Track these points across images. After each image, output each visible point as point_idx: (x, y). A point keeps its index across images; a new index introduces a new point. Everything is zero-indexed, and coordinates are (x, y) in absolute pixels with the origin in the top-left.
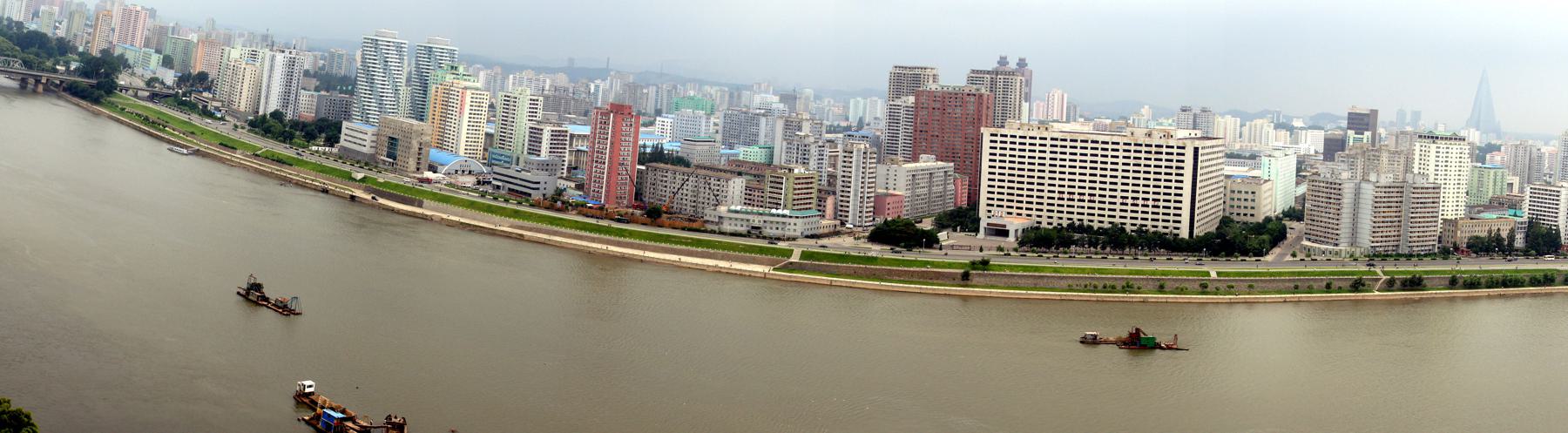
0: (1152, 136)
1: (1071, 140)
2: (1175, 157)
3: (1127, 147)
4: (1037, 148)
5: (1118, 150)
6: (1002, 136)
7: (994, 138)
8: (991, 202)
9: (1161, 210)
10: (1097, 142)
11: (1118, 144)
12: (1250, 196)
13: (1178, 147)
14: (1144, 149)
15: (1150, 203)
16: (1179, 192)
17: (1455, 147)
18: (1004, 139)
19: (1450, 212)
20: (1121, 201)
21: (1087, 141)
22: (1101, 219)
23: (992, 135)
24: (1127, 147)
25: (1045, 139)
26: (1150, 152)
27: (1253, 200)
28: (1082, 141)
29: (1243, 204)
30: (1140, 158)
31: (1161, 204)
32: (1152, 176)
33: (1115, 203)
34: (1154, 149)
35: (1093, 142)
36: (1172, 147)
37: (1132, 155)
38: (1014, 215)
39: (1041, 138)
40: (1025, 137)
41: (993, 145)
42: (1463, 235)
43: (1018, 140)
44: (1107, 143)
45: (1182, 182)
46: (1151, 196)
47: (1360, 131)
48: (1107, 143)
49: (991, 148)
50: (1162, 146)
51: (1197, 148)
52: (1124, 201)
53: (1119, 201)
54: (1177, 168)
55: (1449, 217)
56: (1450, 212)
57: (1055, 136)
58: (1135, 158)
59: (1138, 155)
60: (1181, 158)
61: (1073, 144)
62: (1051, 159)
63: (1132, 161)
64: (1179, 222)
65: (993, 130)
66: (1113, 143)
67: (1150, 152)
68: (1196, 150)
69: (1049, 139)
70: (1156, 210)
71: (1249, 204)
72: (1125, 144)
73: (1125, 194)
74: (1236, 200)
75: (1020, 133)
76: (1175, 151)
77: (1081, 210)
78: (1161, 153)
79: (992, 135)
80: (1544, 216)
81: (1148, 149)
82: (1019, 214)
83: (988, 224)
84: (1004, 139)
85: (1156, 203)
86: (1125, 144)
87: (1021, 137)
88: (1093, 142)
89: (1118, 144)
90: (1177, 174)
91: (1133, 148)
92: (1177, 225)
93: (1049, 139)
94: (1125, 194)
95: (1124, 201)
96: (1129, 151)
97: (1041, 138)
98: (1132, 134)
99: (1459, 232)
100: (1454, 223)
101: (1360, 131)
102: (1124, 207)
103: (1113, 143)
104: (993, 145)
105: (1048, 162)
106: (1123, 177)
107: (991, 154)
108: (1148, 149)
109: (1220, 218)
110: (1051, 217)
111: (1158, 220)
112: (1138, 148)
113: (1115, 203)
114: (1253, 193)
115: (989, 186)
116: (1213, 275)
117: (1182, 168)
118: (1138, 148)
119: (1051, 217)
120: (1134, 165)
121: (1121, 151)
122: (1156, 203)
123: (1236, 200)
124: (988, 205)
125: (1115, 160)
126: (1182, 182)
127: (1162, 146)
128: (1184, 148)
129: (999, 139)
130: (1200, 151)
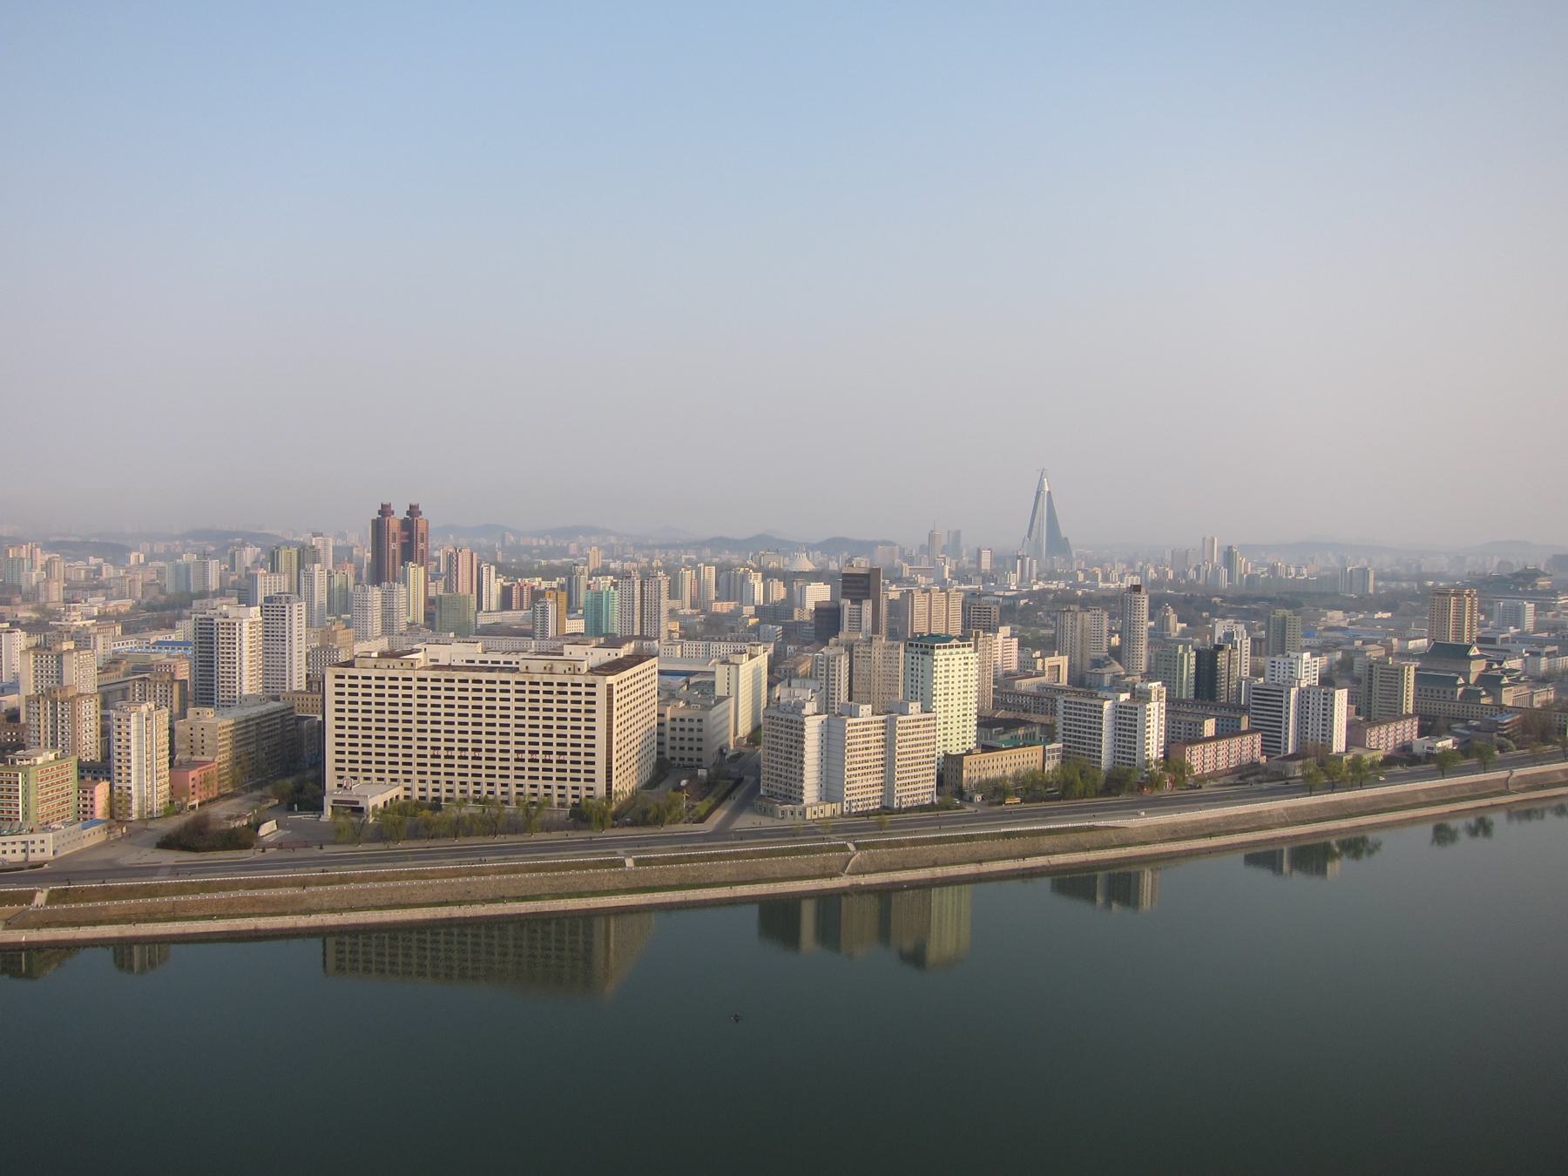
0: (554, 671)
1: (447, 681)
2: (583, 698)
3: (520, 687)
4: (400, 692)
5: (508, 691)
6: (350, 677)
7: (340, 681)
8: (340, 765)
9: (569, 766)
10: (480, 682)
11: (508, 683)
12: (695, 725)
13: (587, 685)
14: (542, 688)
15: (554, 757)
16: (590, 742)
17: (957, 657)
18: (353, 682)
19: (954, 742)
20: (515, 756)
21: (466, 681)
22: (491, 780)
23: (337, 677)
24: (520, 687)
25: (410, 679)
26: (551, 693)
27: (700, 730)
28: (460, 681)
29: (686, 735)
30: (538, 701)
31: (569, 758)
32: (555, 723)
33: (508, 760)
34: (555, 688)
35: (475, 681)
36: (580, 685)
37: (527, 696)
38: (375, 780)
39: (404, 679)
40: (383, 679)
41: (340, 690)
42: (972, 775)
43: (373, 682)
44: (494, 682)
45: (593, 729)
46: (555, 749)
47: (857, 601)
48: (494, 682)
49: (337, 694)
50: (566, 685)
51: (612, 685)
52: (520, 756)
53: (512, 755)
54: (587, 711)
55: (954, 753)
56: (954, 742)
57: (423, 674)
58: (531, 700)
59: (534, 696)
60: (591, 698)
61: (449, 685)
62: (419, 705)
63: (527, 705)
64: (593, 780)
65: (340, 671)
66: (502, 682)
67: (551, 693)
68: (610, 687)
69: (415, 679)
70: (562, 766)
71: (695, 735)
72: (517, 683)
73: (520, 747)
74: (678, 730)
75: (374, 673)
76: (583, 689)
77: (463, 771)
78: (566, 693)
79: (337, 677)
80: (1085, 744)
81: (547, 688)
82: (379, 779)
83: (335, 801)
84: (353, 682)
85: (562, 758)
86: (517, 683)
87: (377, 678)
88: (475, 681)
89: (508, 683)
90: (587, 720)
91: (527, 687)
92: (591, 784)
93: (415, 679)
94: (520, 747)
95: (520, 756)
96: (523, 692)
97: (404, 679)
98: (527, 668)
99: (965, 772)
100: (958, 759)
101: (857, 601)
102: (520, 764)
103: (502, 682)
104: (340, 690)
105: (415, 709)
106: (517, 726)
107: (337, 702)
108: (547, 688)
109: (655, 759)
110: (424, 781)
111: (565, 779)
112: (535, 688)
113: (508, 760)
114: (699, 721)
115: (337, 744)
116: (629, 862)
117: (594, 711)
118: (535, 688)
119: (424, 781)
120: (531, 709)
121: (512, 692)
122: (562, 758)
123: (678, 730)
124: (337, 769)
125: (505, 704)
126: (593, 729)
127: (566, 685)
128: (594, 686)
129: (347, 681)
130: (615, 688)
